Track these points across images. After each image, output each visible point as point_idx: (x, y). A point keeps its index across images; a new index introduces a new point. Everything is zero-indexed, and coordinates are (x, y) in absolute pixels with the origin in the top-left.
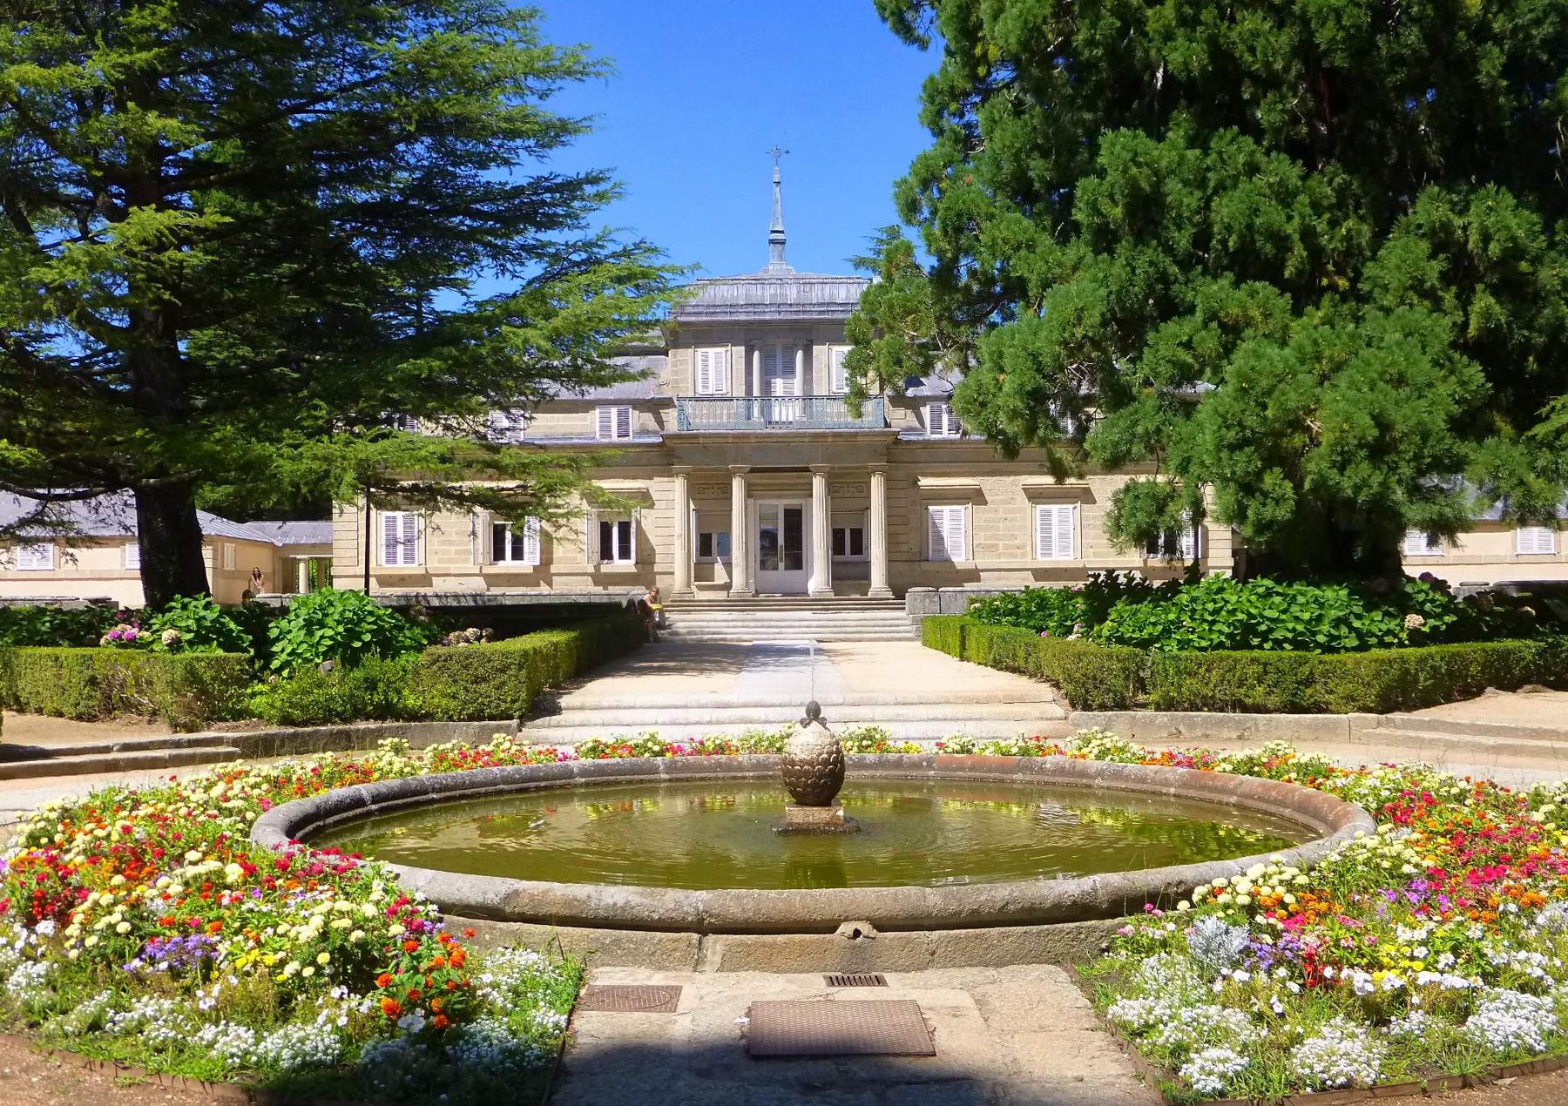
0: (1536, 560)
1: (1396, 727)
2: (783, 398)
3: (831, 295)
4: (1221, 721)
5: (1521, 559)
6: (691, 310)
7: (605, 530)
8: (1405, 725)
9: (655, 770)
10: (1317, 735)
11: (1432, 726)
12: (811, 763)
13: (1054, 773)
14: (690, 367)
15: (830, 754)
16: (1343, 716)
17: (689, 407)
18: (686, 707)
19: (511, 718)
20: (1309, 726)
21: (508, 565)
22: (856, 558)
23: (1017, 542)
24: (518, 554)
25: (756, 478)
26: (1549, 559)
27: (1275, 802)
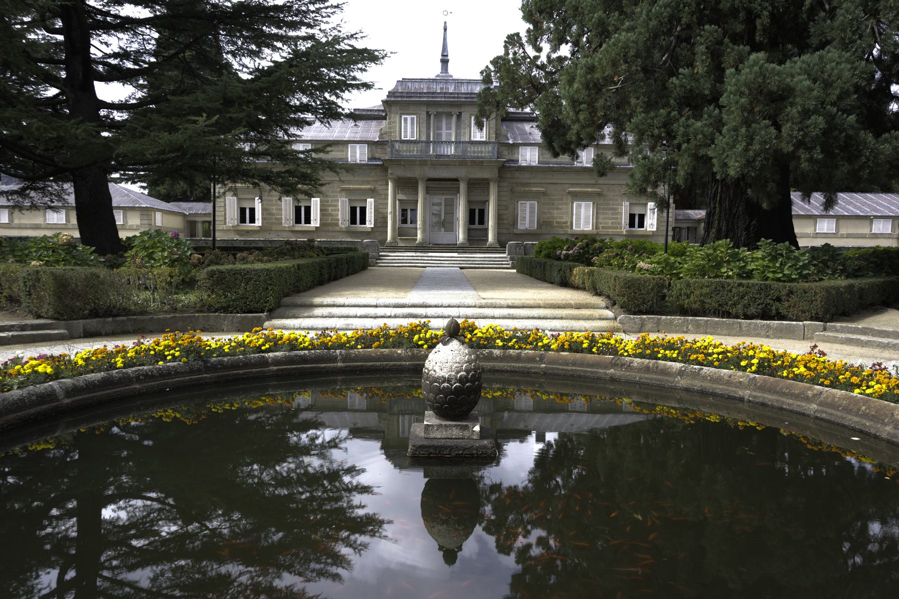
0: (825, 236)
1: (837, 331)
2: (445, 142)
3: (471, 90)
4: (717, 323)
5: (818, 236)
6: (398, 95)
7: (353, 210)
8: (842, 330)
9: (334, 359)
10: (780, 334)
11: (864, 331)
12: (448, 380)
13: (640, 370)
14: (398, 125)
15: (467, 371)
16: (801, 323)
17: (397, 146)
18: (376, 306)
19: (262, 312)
20: (776, 329)
21: (303, 226)
22: (481, 227)
23: (563, 220)
24: (308, 221)
25: (431, 184)
26: (832, 236)
27: (865, 416)
